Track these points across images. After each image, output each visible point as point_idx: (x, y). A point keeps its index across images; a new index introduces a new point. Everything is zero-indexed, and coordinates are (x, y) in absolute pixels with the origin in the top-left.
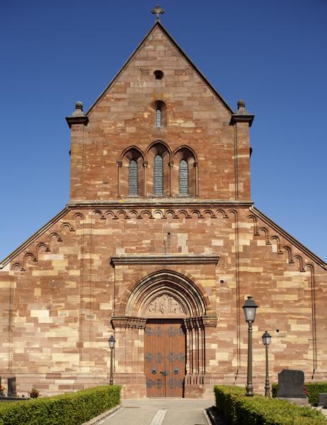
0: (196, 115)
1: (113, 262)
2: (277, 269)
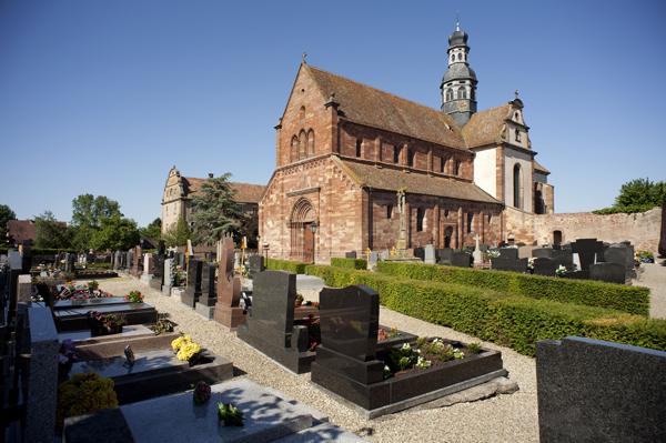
0: (315, 109)
1: (289, 195)
2: (342, 190)
